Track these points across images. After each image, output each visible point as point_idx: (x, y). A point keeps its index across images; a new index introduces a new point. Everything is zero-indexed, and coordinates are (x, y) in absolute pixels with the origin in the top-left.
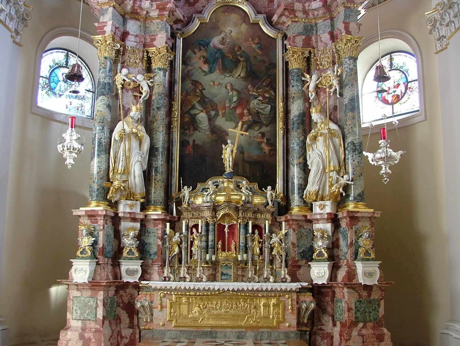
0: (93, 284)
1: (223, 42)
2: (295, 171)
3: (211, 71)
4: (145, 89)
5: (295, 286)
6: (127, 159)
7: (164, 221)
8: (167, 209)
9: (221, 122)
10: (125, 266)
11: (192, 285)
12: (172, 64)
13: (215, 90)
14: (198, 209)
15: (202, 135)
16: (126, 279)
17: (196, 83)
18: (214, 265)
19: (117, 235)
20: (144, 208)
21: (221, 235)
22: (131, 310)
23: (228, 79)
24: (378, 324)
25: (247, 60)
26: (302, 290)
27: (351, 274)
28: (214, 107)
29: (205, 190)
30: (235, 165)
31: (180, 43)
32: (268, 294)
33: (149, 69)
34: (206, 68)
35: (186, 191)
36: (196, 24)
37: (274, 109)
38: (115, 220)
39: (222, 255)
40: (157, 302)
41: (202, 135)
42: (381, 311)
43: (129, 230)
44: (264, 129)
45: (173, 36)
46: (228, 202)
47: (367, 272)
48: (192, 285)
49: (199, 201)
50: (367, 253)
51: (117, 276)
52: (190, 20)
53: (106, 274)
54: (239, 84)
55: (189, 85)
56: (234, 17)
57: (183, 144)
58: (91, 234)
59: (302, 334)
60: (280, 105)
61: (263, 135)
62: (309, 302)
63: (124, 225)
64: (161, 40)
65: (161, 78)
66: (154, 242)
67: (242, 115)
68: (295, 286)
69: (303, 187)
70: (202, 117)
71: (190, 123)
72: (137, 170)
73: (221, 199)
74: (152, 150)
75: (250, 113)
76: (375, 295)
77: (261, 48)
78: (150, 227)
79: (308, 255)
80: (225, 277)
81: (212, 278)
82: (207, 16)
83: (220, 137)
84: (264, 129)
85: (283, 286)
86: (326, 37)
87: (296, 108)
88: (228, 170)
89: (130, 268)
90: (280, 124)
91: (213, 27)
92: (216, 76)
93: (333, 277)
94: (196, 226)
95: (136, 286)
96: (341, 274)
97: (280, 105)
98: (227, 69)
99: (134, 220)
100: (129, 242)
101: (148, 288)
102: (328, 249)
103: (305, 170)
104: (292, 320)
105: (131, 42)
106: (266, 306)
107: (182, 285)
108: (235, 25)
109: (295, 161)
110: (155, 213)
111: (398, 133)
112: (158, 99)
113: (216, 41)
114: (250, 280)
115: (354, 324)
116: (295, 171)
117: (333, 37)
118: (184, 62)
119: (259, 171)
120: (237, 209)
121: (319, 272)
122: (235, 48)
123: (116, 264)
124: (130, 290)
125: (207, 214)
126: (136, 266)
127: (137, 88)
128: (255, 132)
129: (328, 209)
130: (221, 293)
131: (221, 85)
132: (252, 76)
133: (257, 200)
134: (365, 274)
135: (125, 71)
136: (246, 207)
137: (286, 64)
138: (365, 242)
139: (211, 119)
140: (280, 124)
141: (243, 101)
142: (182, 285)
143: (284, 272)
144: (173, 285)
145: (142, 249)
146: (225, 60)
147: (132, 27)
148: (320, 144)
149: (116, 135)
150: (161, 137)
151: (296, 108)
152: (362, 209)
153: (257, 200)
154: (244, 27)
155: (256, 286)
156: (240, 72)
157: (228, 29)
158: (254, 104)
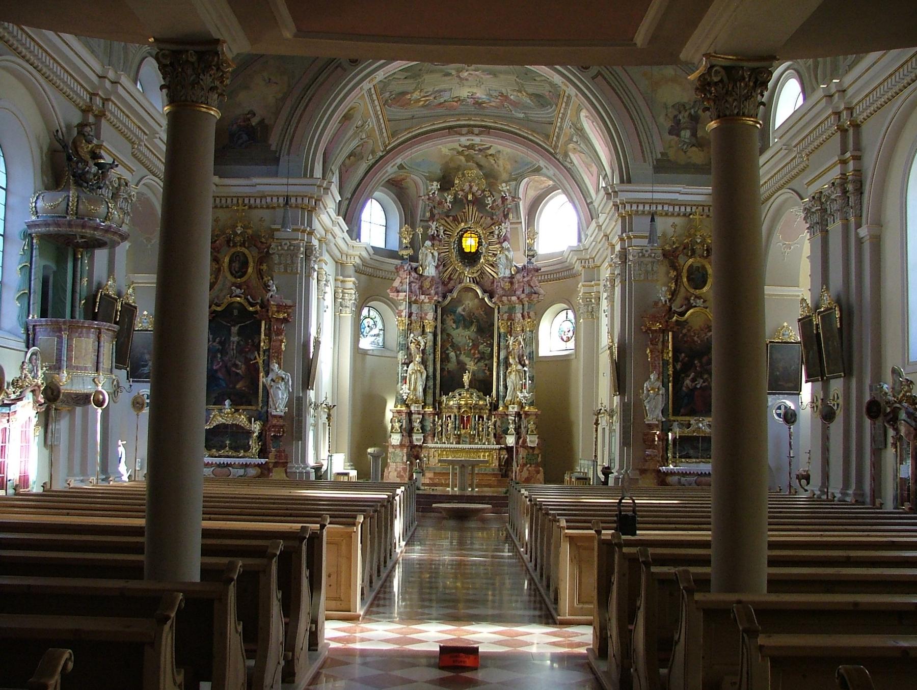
0: (401, 445)
1: (464, 310)
2: (501, 388)
4: (423, 344)
5: (499, 446)
6: (416, 383)
7: (434, 414)
8: (434, 408)
9: (463, 358)
10: (415, 437)
11: (449, 446)
12: (436, 327)
13: (459, 339)
14: (451, 408)
15: (452, 365)
16: (416, 443)
17: (448, 335)
18: (459, 436)
19: (410, 421)
20: (423, 407)
21: (462, 421)
22: (417, 457)
23: (467, 333)
24: (537, 465)
25: (478, 321)
26: (501, 448)
27: (525, 441)
28: (459, 350)
29: (454, 397)
30: (470, 382)
32: (485, 450)
33: (423, 333)
35: (444, 398)
36: (449, 298)
37: (492, 350)
38: (410, 414)
39: (463, 432)
40: (431, 454)
41: (452, 365)
42: (539, 459)
43: (417, 418)
44: (487, 362)
45: (436, 312)
46: (466, 404)
47: (532, 440)
48: (449, 446)
49: (451, 403)
50: (532, 431)
51: (411, 442)
52: (445, 297)
53: (406, 441)
54: (473, 336)
55: (445, 336)
56: (471, 294)
57: (442, 369)
58: (399, 421)
59: (501, 470)
60: (495, 349)
62: (505, 455)
63: (414, 416)
64: (430, 316)
65: (430, 337)
66: (429, 425)
67: (474, 354)
68: (499, 446)
69: (505, 397)
70: (452, 354)
71: (445, 359)
72: (420, 389)
73: (463, 403)
74: (427, 377)
75: (479, 352)
76: (536, 452)
77: (486, 314)
78: (427, 417)
79: (506, 432)
80: (465, 442)
81: (458, 443)
82: (455, 295)
83: (462, 368)
84: (487, 362)
85: (492, 447)
86: (519, 315)
87: (503, 355)
88: (467, 387)
89: (417, 438)
90: (495, 359)
91: (458, 301)
92: (460, 330)
93: (517, 443)
94: (450, 417)
95: (420, 447)
96: (521, 441)
97: (495, 349)
98: (467, 327)
99: (419, 414)
100: (417, 425)
101: (426, 447)
102: (515, 429)
103: (506, 387)
104: (495, 464)
105: (414, 317)
106: (484, 456)
107: (444, 446)
108: (471, 300)
110: (429, 410)
111: (561, 363)
112: (429, 349)
113: (460, 310)
114: (477, 444)
115: (525, 465)
116: (501, 388)
117: (523, 316)
119: (483, 385)
120: (471, 408)
121: (511, 440)
122: (471, 314)
123: (410, 436)
124: (417, 449)
125: (456, 410)
126: (421, 436)
127: (418, 343)
128: (481, 364)
129: (516, 410)
130: (463, 450)
131: (463, 336)
132: (480, 331)
133: (481, 403)
134: (530, 441)
135: (412, 335)
136: (476, 406)
137: (498, 328)
138: (531, 426)
140: (495, 359)
141: (475, 346)
142: (444, 446)
143: (493, 440)
144: (440, 446)
145: (423, 428)
146: (465, 321)
147: (414, 307)
148: (513, 376)
149: (410, 371)
150: (431, 370)
151: (503, 355)
152: (533, 410)
153: (481, 403)
154: (476, 301)
155: (479, 446)
156: (474, 328)
157: (467, 302)
158: (481, 347)
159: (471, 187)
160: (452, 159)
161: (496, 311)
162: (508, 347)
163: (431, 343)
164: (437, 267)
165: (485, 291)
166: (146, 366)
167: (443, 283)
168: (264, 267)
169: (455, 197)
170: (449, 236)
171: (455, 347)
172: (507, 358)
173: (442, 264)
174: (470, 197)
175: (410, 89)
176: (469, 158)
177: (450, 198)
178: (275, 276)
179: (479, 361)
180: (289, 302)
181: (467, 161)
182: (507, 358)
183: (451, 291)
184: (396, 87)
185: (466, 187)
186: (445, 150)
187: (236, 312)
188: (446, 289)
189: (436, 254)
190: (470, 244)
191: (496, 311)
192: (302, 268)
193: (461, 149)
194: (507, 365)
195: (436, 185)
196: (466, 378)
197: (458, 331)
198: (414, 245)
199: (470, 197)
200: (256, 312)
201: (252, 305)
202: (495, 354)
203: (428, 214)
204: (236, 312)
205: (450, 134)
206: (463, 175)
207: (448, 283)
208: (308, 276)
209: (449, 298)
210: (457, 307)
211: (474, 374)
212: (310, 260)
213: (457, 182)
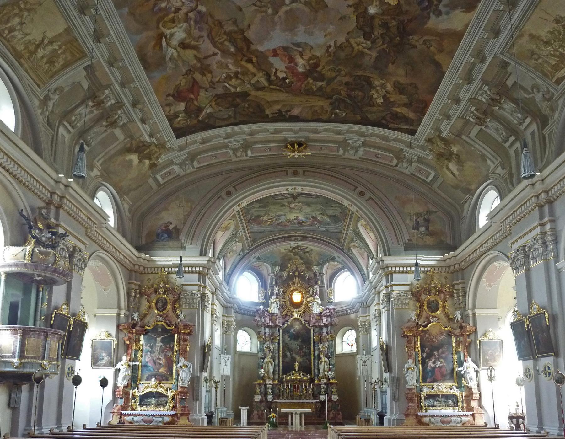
1: (294, 331)
3: (291, 340)
9: (294, 355)
13: (292, 346)
17: (286, 344)
23: (296, 342)
28: (292, 351)
30: (299, 369)
31: (281, 331)
34: (289, 339)
36: (286, 325)
52: (284, 324)
56: (298, 323)
60: (312, 350)
61: (307, 359)
70: (288, 353)
82: (289, 323)
83: (294, 360)
87: (317, 353)
97: (312, 350)
109: (316, 368)
113: (292, 331)
118: (282, 337)
128: (305, 358)
139: (291, 354)
141: (301, 349)
151: (317, 353)
154: (301, 326)
156: (300, 340)
158: (304, 349)
159: (297, 268)
160: (286, 255)
161: (312, 331)
162: (319, 349)
163: (277, 348)
164: (279, 309)
165: (306, 321)
166: (103, 359)
167: (283, 318)
168: (177, 305)
169: (288, 274)
170: (285, 293)
171: (290, 350)
172: (319, 355)
173: (282, 307)
174: (296, 273)
175: (262, 214)
176: (296, 254)
177: (285, 274)
178: (183, 310)
179: (303, 356)
180: (191, 324)
181: (295, 255)
182: (319, 355)
183: (287, 321)
184: (254, 212)
185: (294, 268)
186: (282, 250)
187: (159, 330)
188: (284, 320)
189: (279, 302)
190: (297, 297)
191: (312, 331)
192: (199, 305)
193: (291, 249)
194: (319, 358)
195: (277, 268)
196: (296, 365)
197: (291, 342)
198: (267, 298)
199: (296, 273)
200: (172, 330)
201: (169, 326)
202: (312, 353)
203: (274, 283)
204: (159, 330)
205: (285, 241)
206: (293, 262)
207: (286, 317)
208: (203, 310)
209: (286, 325)
210: (290, 330)
211: (300, 363)
212: (204, 302)
213: (289, 266)
